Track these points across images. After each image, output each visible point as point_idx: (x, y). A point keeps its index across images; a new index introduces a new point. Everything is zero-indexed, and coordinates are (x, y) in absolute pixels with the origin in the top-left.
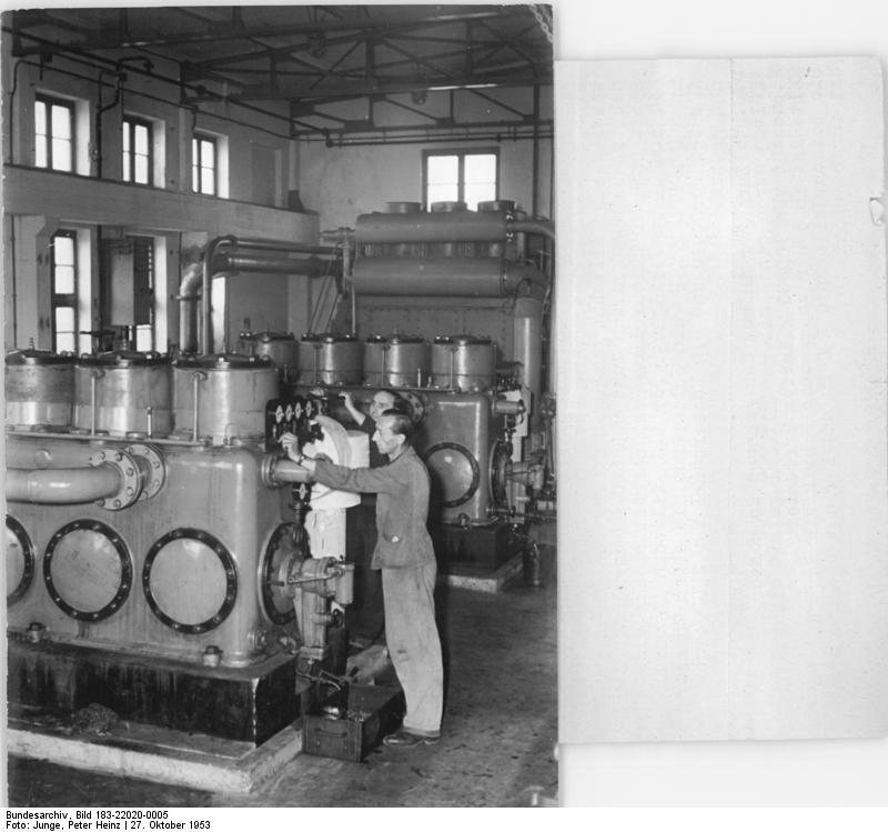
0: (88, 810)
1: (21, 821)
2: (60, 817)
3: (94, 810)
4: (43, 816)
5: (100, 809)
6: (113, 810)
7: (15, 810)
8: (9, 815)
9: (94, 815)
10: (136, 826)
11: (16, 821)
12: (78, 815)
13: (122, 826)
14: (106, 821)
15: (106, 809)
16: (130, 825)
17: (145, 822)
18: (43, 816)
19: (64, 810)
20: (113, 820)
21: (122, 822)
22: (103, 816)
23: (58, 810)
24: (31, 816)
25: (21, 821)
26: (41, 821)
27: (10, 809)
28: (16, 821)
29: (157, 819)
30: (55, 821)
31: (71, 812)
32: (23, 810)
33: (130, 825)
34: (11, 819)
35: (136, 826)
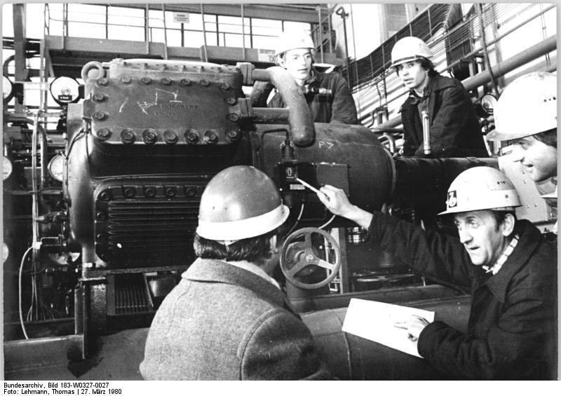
0: (55, 382)
1: (14, 389)
2: (38, 386)
3: (59, 382)
4: (27, 386)
5: (63, 382)
6: (72, 382)
7: (9, 382)
8: (5, 385)
9: (59, 385)
10: (85, 392)
11: (10, 389)
12: (50, 385)
13: (76, 392)
14: (67, 389)
15: (67, 382)
16: (81, 392)
17: (90, 390)
18: (27, 386)
19: (41, 382)
20: (72, 388)
21: (76, 390)
22: (65, 386)
23: (36, 382)
24: (20, 386)
25: (14, 389)
26: (25, 389)
27: (6, 381)
28: (10, 389)
29: (99, 388)
30: (34, 389)
31: (45, 383)
32: (14, 382)
33: (81, 392)
34: (7, 388)
35: (85, 392)
